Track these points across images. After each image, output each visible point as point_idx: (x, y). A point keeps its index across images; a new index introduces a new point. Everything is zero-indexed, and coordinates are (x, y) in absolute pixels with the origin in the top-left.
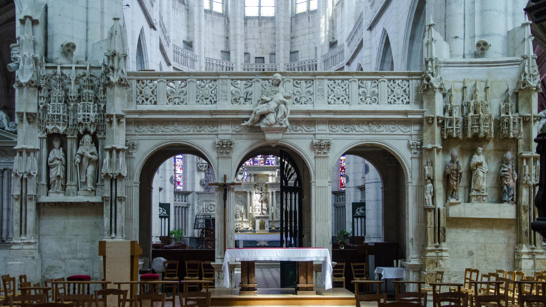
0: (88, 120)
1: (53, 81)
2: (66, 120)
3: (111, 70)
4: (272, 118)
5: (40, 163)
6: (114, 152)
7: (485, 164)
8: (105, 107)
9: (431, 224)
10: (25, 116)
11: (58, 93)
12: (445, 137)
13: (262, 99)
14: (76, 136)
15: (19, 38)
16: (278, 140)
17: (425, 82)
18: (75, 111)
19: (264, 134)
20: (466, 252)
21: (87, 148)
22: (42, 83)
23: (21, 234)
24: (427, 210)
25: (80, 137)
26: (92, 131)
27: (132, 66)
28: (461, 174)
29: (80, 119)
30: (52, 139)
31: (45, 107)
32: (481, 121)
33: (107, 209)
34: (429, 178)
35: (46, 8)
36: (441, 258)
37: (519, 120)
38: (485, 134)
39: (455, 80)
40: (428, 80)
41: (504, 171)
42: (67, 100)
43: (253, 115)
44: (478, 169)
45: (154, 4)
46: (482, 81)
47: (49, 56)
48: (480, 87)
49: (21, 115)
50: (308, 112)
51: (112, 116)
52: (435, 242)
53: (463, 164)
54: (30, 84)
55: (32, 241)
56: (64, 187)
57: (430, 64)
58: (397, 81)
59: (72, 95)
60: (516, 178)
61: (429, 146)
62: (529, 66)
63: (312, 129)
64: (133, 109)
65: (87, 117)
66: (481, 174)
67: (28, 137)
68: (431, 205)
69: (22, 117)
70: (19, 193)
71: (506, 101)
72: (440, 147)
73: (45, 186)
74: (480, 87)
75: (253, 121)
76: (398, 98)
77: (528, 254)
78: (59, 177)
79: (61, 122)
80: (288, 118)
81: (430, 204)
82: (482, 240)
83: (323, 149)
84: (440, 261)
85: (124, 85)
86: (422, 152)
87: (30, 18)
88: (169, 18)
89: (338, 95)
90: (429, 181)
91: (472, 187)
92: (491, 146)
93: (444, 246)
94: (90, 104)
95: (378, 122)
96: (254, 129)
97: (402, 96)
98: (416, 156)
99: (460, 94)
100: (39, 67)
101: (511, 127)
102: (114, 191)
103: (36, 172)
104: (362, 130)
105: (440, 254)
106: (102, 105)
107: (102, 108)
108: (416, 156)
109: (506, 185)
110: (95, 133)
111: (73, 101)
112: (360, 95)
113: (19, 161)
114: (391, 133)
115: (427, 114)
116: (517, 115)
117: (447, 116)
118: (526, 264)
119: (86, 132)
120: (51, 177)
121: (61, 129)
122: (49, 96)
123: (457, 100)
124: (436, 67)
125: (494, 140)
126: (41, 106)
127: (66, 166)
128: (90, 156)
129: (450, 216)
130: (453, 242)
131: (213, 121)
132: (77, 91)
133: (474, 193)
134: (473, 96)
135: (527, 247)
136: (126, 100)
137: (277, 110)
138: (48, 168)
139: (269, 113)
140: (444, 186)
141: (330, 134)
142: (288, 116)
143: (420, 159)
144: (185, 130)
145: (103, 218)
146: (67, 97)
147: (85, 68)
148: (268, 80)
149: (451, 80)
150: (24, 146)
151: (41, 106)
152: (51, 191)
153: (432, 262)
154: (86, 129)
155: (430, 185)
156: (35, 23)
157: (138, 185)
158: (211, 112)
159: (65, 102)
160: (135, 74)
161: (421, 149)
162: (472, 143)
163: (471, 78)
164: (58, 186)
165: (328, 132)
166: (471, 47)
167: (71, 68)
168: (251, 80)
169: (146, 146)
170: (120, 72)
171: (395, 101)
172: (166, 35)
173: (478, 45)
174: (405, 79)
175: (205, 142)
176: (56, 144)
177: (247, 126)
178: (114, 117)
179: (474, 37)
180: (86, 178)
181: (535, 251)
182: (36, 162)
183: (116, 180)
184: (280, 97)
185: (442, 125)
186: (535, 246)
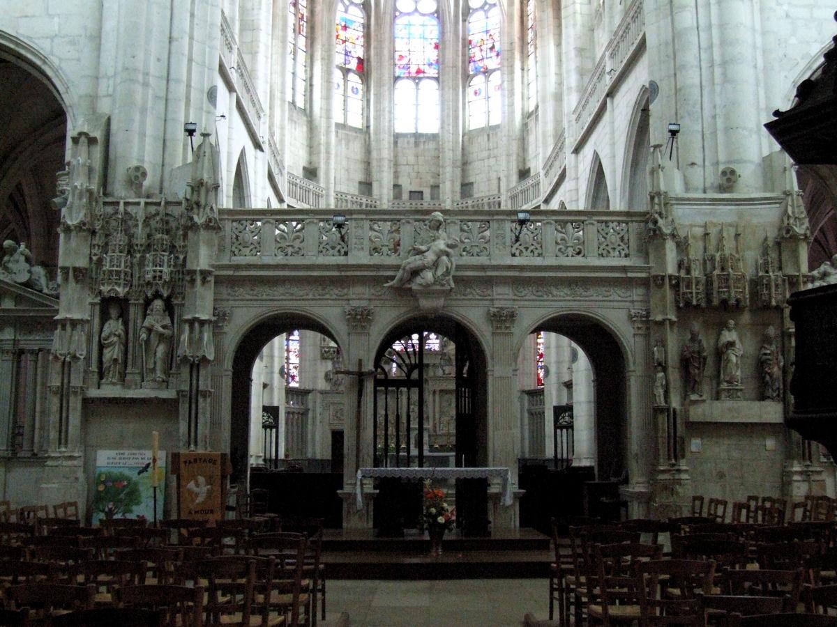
0: (161, 277)
1: (114, 223)
2: (129, 278)
3: (195, 206)
4: (428, 276)
5: (89, 340)
6: (197, 325)
7: (738, 345)
8: (185, 258)
9: (664, 431)
10: (71, 274)
11: (119, 239)
12: (681, 305)
13: (414, 249)
14: (141, 301)
15: (69, 164)
16: (436, 310)
17: (651, 225)
18: (142, 263)
19: (417, 300)
21: (156, 320)
22: (98, 225)
23: (60, 443)
24: (658, 411)
25: (148, 303)
26: (165, 294)
27: (226, 200)
28: (705, 358)
29: (149, 277)
30: (109, 306)
31: (100, 261)
32: (731, 282)
33: (184, 408)
34: (660, 364)
35: (109, 119)
36: (679, 482)
37: (784, 281)
38: (738, 301)
40: (655, 222)
41: (765, 354)
43: (401, 271)
44: (729, 351)
45: (262, 115)
46: (730, 225)
47: (109, 189)
48: (729, 234)
49: (65, 270)
50: (483, 268)
51: (195, 272)
52: (669, 459)
53: (707, 343)
54: (80, 227)
55: (76, 455)
56: (123, 376)
57: (656, 200)
58: (611, 225)
59: (139, 242)
60: (782, 364)
61: (659, 318)
62: (793, 206)
63: (489, 292)
64: (226, 262)
65: (158, 274)
66: (734, 359)
67: (75, 304)
68: (663, 404)
69: (67, 273)
70: (59, 384)
71: (765, 253)
72: (674, 319)
73: (96, 374)
74: (729, 234)
75: (401, 280)
76: (614, 249)
77: (801, 473)
78: (115, 360)
80: (454, 277)
81: (661, 401)
82: (735, 454)
83: (505, 321)
85: (213, 228)
86: (649, 326)
87: (86, 134)
88: (283, 135)
89: (526, 243)
90: (660, 368)
91: (722, 376)
92: (746, 318)
93: (683, 465)
94: (163, 256)
95: (586, 282)
96: (403, 291)
97: (619, 245)
98: (640, 332)
99: (701, 244)
100: (94, 204)
101: (773, 290)
102: (194, 382)
103: (84, 353)
104: (562, 294)
106: (181, 257)
107: (180, 261)
108: (640, 332)
109: (769, 374)
110: (169, 297)
111: (139, 251)
112: (557, 243)
113: (61, 338)
114: (605, 299)
115: (654, 273)
116: (780, 273)
117: (683, 274)
118: (799, 488)
119: (157, 295)
120: (104, 360)
121: (121, 291)
122: (107, 244)
123: (696, 252)
124: (666, 204)
125: (750, 311)
126: (95, 258)
127: (126, 345)
128: (161, 329)
129: (691, 420)
131: (342, 279)
132: (145, 236)
133: (724, 386)
134: (720, 247)
136: (216, 248)
137: (435, 265)
138: (101, 348)
139: (423, 268)
140: (681, 377)
141: (514, 300)
142: (453, 273)
143: (647, 336)
144: (301, 293)
145: (178, 423)
146: (130, 245)
147: (159, 204)
148: (424, 221)
149: (687, 223)
150: (68, 316)
151: (95, 258)
152: (104, 381)
153: (665, 488)
154: (157, 292)
155: (661, 375)
156: (92, 141)
157: (230, 373)
158: (339, 267)
159: (129, 252)
160: (229, 212)
161: (648, 322)
162: (720, 311)
163: (715, 220)
164: (113, 376)
165: (511, 296)
166: (712, 178)
167: (138, 204)
168: (399, 221)
169: (243, 317)
170: (208, 209)
171: (609, 252)
172: (278, 158)
173: (724, 173)
174: (623, 222)
175: (330, 311)
176: (114, 312)
177: (391, 287)
178: (198, 273)
179: (717, 163)
180: (155, 363)
181: (811, 469)
182: (84, 338)
184: (441, 245)
185: (676, 287)
186: (811, 462)
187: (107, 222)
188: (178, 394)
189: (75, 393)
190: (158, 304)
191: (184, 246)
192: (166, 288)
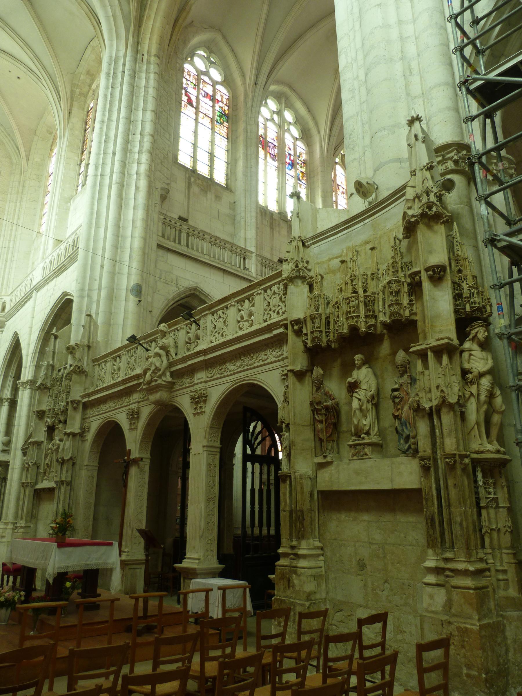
20: (354, 563)
39: (331, 257)
77: (438, 571)
82: (378, 536)
84: (294, 576)
97: (279, 306)
105: (295, 563)
118: (431, 597)
130: (335, 539)
135: (437, 555)
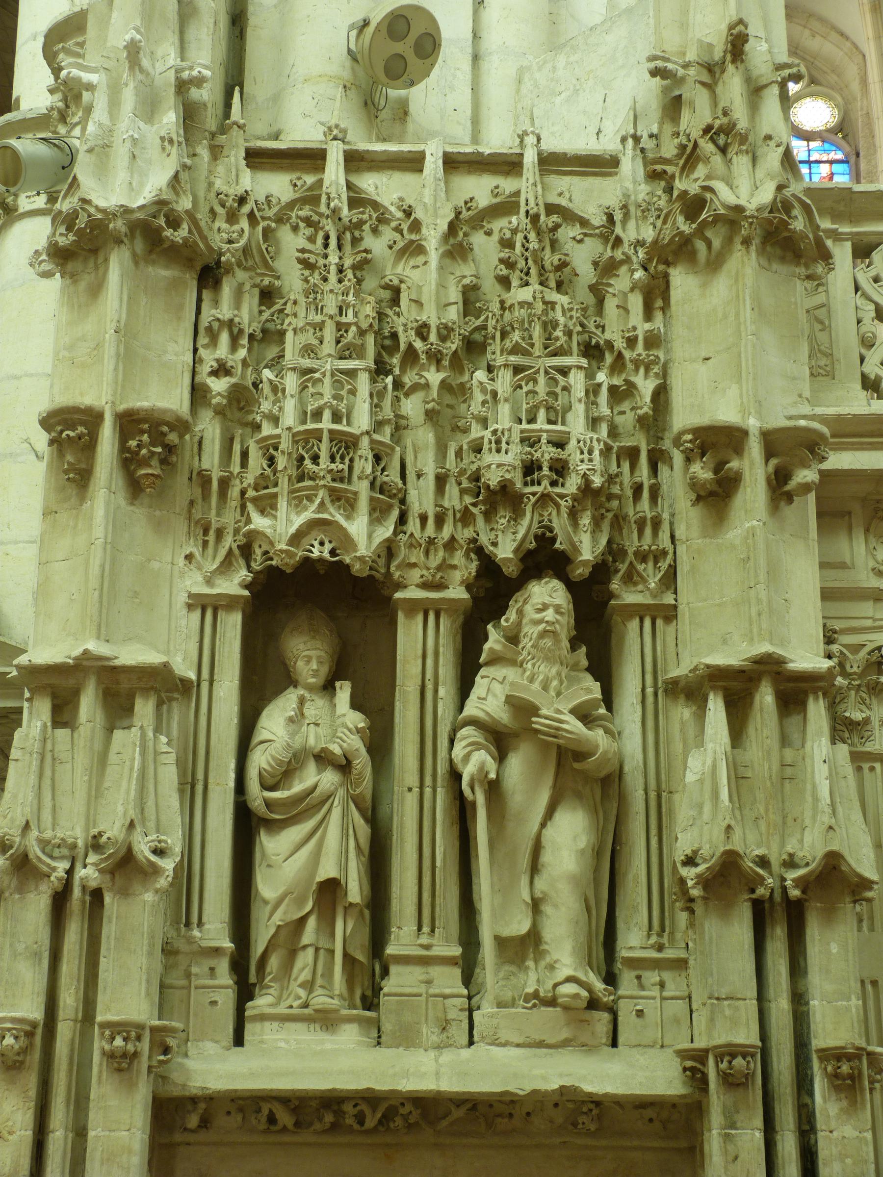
0: (560, 469)
5: (192, 788)
6: (766, 697)
8: (661, 394)
10: (107, 434)
14: (457, 592)
25: (494, 590)
26: (588, 549)
29: (500, 466)
31: (241, 400)
42: (390, 356)
65: (546, 453)
69: (89, 446)
70: (35, 1012)
73: (223, 966)
78: (330, 891)
79: (362, 488)
94: (564, 371)
100: (204, 153)
103: (175, 841)
106: (646, 386)
110: (602, 571)
121: (363, 535)
126: (219, 386)
128: (574, 725)
138: (247, 826)
150: (93, 646)
151: (219, 386)
152: (261, 1003)
154: (545, 539)
164: (314, 974)
176: (308, 654)
183: (795, 916)
187: (267, 233)
188: (696, 1076)
189: (122, 1063)
190: (545, 601)
191: (653, 341)
192: (586, 520)
